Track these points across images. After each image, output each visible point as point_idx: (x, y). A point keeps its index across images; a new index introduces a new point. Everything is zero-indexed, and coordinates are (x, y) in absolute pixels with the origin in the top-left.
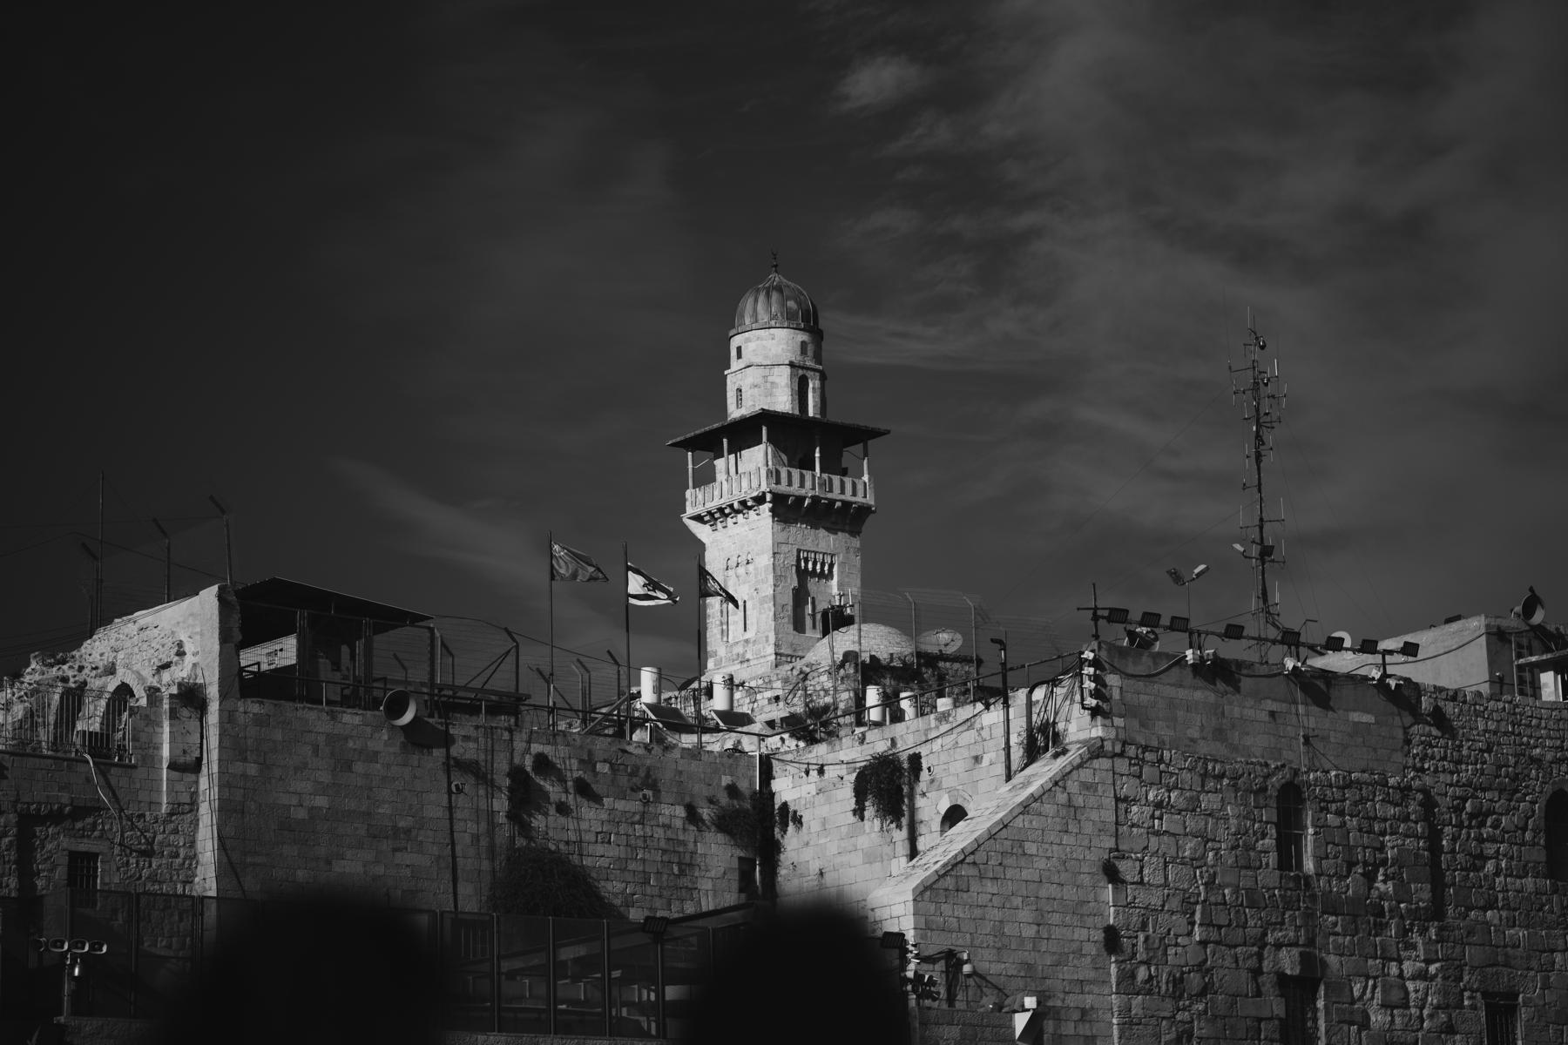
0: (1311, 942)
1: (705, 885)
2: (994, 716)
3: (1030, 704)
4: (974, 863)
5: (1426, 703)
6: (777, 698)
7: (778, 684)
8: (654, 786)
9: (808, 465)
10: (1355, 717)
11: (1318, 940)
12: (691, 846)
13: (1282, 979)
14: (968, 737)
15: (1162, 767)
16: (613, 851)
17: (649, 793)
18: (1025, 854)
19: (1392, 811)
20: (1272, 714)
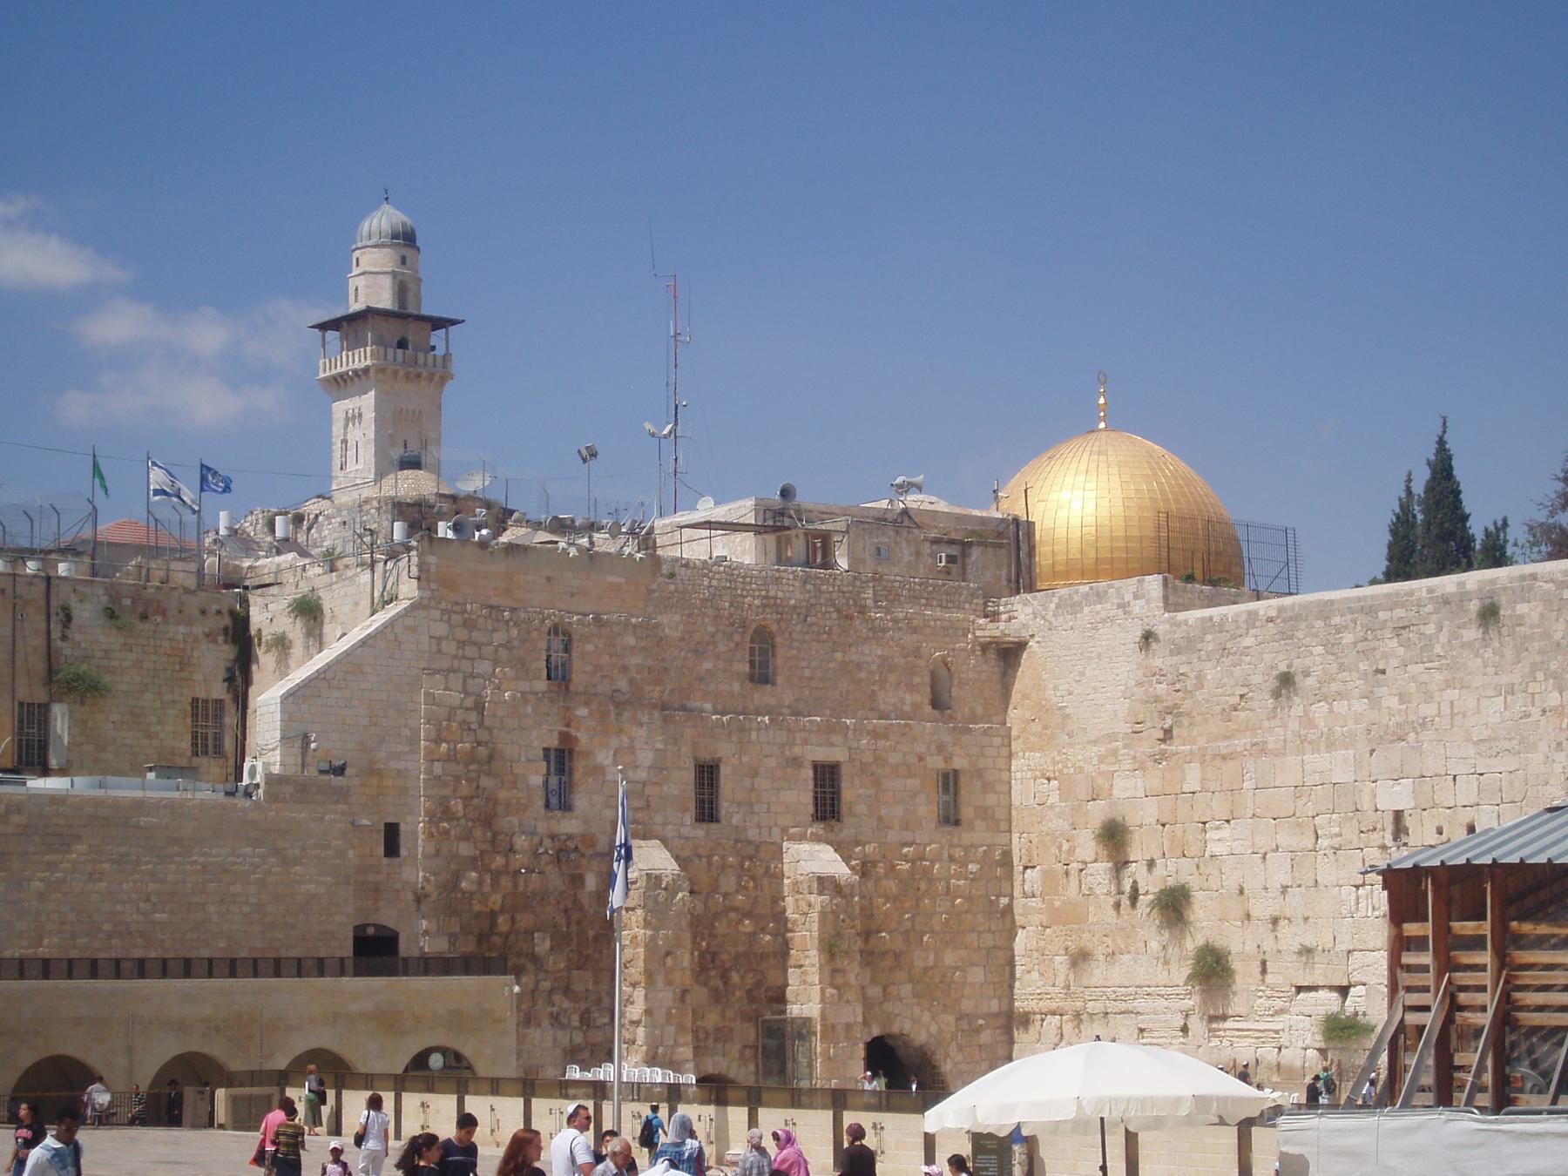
0: (568, 725)
1: (198, 677)
2: (366, 577)
3: (385, 571)
4: (325, 679)
5: (665, 569)
6: (345, 523)
7: (345, 513)
8: (163, 613)
9: (402, 344)
10: (610, 579)
11: (573, 724)
12: (189, 652)
13: (546, 750)
14: (351, 590)
15: (466, 616)
16: (133, 656)
17: (159, 619)
18: (362, 673)
19: (631, 641)
20: (549, 579)
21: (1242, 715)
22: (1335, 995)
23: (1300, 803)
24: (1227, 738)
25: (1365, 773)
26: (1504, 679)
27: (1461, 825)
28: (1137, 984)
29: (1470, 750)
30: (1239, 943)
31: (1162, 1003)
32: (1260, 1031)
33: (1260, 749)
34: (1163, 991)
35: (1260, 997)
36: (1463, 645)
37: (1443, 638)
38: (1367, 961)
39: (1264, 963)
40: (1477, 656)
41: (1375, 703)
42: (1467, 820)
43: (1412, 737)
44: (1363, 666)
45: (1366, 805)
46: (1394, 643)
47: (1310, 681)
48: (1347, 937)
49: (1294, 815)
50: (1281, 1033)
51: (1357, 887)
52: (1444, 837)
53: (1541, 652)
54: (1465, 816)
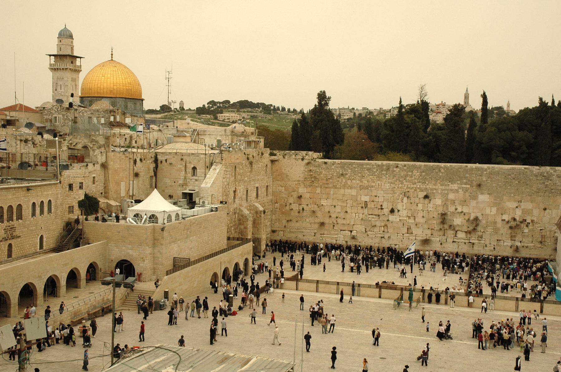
14: (197, 158)
21: (331, 180)
22: (350, 232)
24: (327, 184)
26: (390, 181)
29: (382, 192)
30: (327, 221)
31: (309, 231)
33: (335, 187)
36: (382, 174)
37: (378, 172)
39: (334, 226)
40: (385, 176)
41: (362, 182)
43: (370, 189)
44: (359, 175)
45: (359, 199)
46: (367, 172)
47: (347, 176)
48: (353, 222)
53: (398, 177)
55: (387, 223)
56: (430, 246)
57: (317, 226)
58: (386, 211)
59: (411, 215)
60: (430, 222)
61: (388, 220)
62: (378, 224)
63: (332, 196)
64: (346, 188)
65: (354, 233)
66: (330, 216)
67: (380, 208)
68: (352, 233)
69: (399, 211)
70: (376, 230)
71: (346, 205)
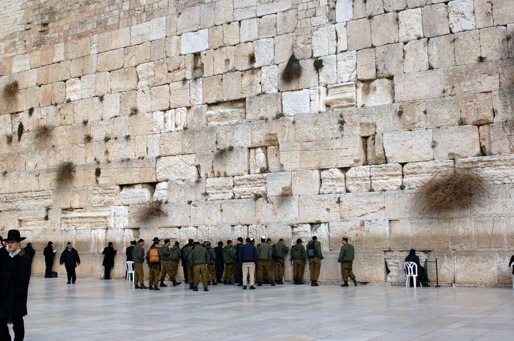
22: (146, 192)
23: (127, 58)
25: (173, 30)
27: (243, 56)
28: (19, 191)
30: (82, 157)
31: (32, 203)
32: (94, 218)
33: (103, 26)
34: (34, 194)
35: (95, 194)
38: (171, 163)
39: (98, 172)
42: (249, 52)
45: (173, 52)
48: (157, 148)
49: (123, 67)
50: (108, 218)
51: (165, 111)
52: (230, 67)
54: (247, 50)
55: (275, 128)
56: (478, 210)
57: (48, 182)
58: (270, 77)
59: (371, 74)
60: (465, 87)
61: (280, 116)
62: (242, 138)
63: (94, 61)
64: (134, 19)
65: (161, 192)
66: (88, 139)
67: (246, 67)
68: (155, 195)
69: (318, 65)
70: (236, 165)
71: (132, 84)
